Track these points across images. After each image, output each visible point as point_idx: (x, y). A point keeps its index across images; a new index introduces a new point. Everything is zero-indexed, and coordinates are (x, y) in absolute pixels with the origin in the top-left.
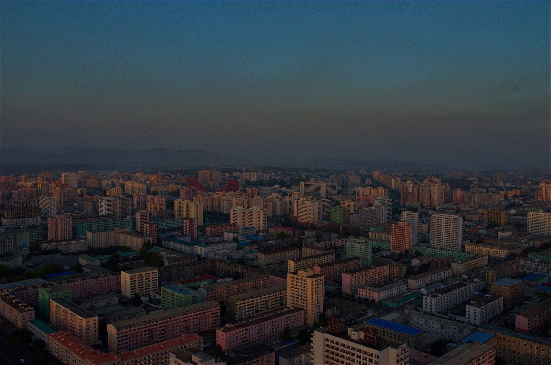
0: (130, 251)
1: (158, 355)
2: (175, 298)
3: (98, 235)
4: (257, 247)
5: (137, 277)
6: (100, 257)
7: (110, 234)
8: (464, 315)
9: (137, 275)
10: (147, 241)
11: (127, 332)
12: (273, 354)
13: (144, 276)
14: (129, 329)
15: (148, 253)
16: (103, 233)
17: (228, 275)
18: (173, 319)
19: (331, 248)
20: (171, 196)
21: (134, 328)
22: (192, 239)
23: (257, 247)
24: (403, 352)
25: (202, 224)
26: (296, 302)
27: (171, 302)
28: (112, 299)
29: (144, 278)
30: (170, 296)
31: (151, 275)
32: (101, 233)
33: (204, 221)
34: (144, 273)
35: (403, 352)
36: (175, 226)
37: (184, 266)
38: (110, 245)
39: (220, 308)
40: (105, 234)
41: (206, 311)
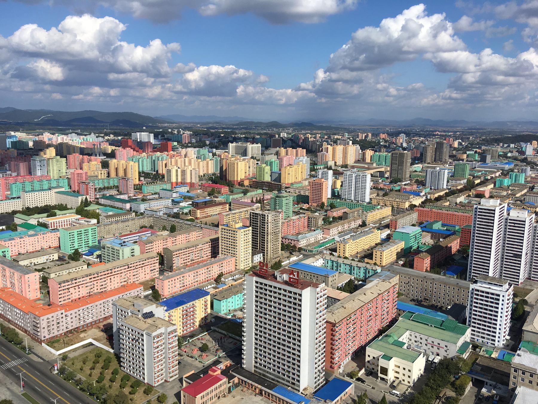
0: (66, 210)
1: (101, 304)
2: (115, 251)
3: (33, 195)
4: (191, 203)
5: (76, 234)
6: (36, 216)
7: (45, 193)
8: (372, 259)
9: (75, 231)
10: (84, 199)
11: (69, 285)
12: (208, 298)
13: (83, 232)
14: (70, 283)
15: (86, 210)
16: (37, 193)
17: (164, 229)
18: (113, 271)
19: (256, 203)
20: (105, 157)
21: (76, 281)
22: (129, 197)
23: (191, 203)
24: (322, 291)
25: (137, 182)
26: (228, 251)
27: (111, 255)
28: (51, 255)
29: (83, 234)
30: (110, 249)
31: (90, 231)
32: (36, 193)
33: (139, 180)
34: (83, 230)
35: (322, 291)
36: (112, 184)
37: (122, 222)
38: (46, 204)
39: (158, 258)
40: (40, 194)
41: (145, 262)
